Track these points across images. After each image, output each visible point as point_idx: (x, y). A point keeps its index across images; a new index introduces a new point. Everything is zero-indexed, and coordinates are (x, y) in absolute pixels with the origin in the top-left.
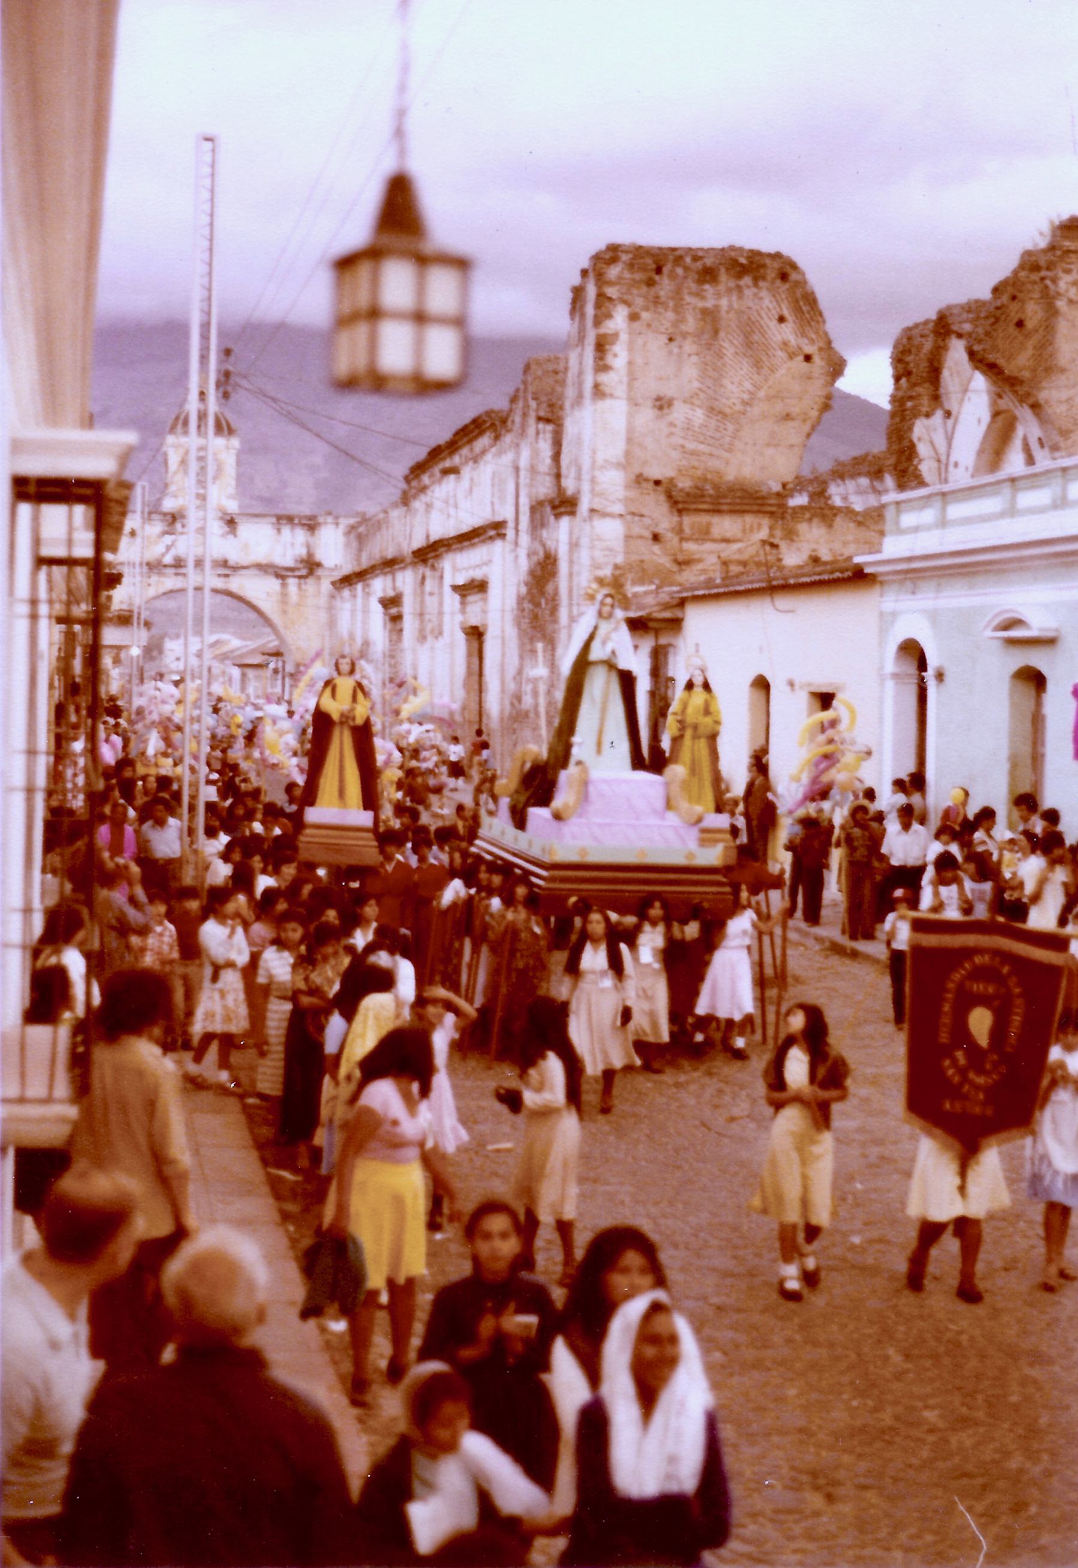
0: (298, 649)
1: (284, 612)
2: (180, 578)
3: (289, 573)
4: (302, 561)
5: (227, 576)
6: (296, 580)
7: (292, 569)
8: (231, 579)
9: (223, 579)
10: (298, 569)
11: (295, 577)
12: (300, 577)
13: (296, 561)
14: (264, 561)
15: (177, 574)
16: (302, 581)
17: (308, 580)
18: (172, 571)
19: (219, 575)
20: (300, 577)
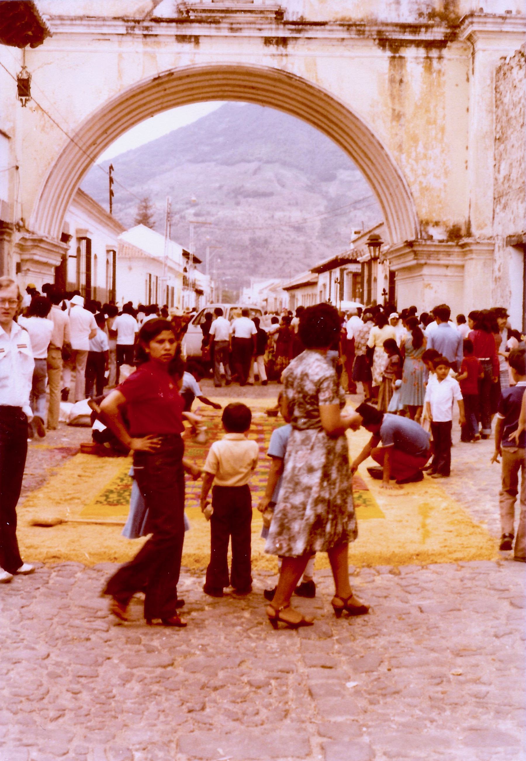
0: (425, 190)
1: (397, 116)
2: (188, 47)
3: (408, 36)
4: (432, 15)
5: (283, 41)
6: (422, 52)
7: (415, 28)
8: (291, 48)
9: (273, 49)
10: (427, 27)
11: (418, 44)
12: (429, 45)
13: (421, 15)
14: (356, 15)
15: (182, 38)
16: (434, 53)
17: (445, 52)
18: (173, 30)
19: (268, 41)
20: (429, 45)
